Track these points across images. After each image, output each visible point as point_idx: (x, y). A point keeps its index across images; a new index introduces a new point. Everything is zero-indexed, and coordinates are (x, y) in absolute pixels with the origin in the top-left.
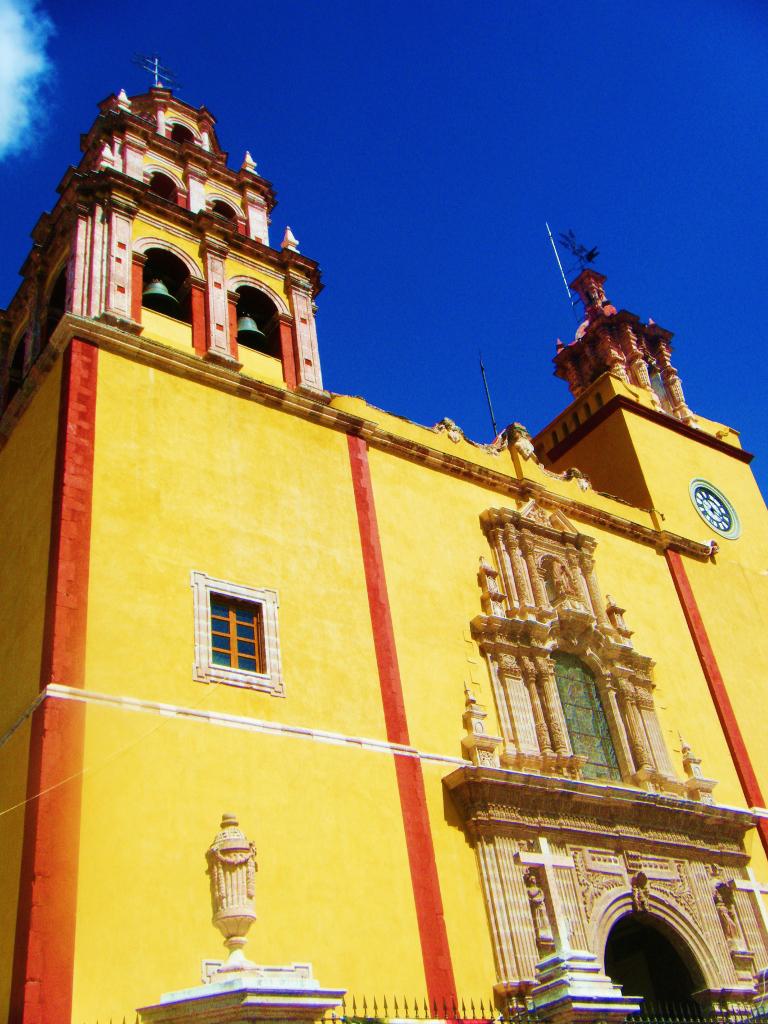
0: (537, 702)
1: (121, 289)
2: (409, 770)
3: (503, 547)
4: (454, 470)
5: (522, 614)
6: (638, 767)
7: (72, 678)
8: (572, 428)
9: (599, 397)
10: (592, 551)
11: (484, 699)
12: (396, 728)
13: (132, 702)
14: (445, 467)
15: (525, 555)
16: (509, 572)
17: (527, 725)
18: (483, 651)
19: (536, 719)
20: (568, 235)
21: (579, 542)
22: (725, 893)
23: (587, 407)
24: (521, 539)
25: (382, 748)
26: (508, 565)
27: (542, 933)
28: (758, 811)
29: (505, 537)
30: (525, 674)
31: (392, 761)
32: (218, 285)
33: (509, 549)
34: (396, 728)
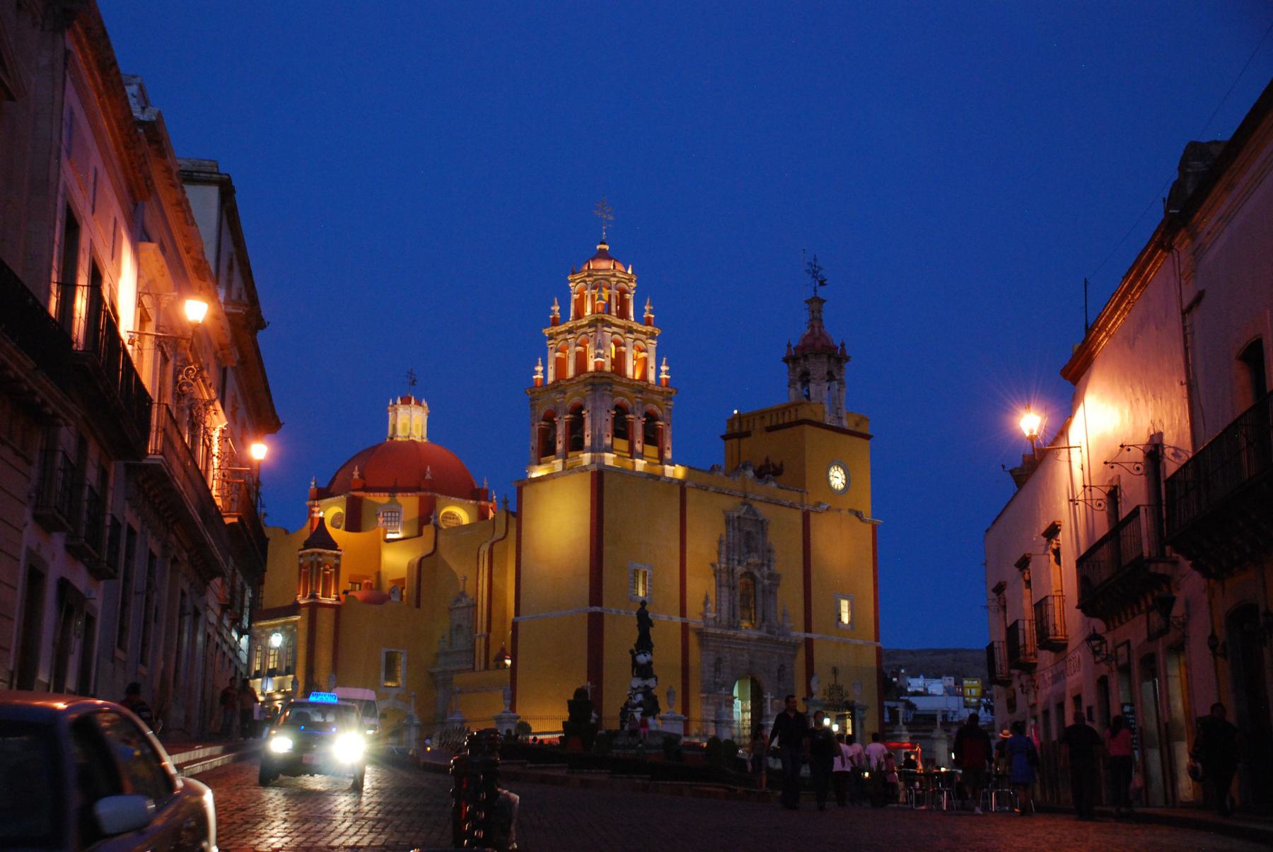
0: (731, 598)
1: (608, 436)
2: (685, 627)
3: (731, 530)
4: (718, 493)
5: (733, 559)
6: (763, 620)
7: (600, 604)
8: (781, 422)
9: (796, 410)
10: (767, 523)
11: (712, 597)
12: (683, 613)
13: (614, 610)
14: (715, 491)
15: (740, 530)
16: (731, 541)
17: (725, 608)
18: (715, 576)
19: (729, 604)
20: (812, 261)
21: (762, 522)
22: (782, 669)
23: (790, 411)
24: (739, 524)
25: (677, 619)
26: (731, 538)
27: (717, 680)
28: (808, 635)
29: (733, 524)
30: (729, 586)
31: (680, 624)
32: (639, 418)
33: (734, 529)
34: (683, 613)
